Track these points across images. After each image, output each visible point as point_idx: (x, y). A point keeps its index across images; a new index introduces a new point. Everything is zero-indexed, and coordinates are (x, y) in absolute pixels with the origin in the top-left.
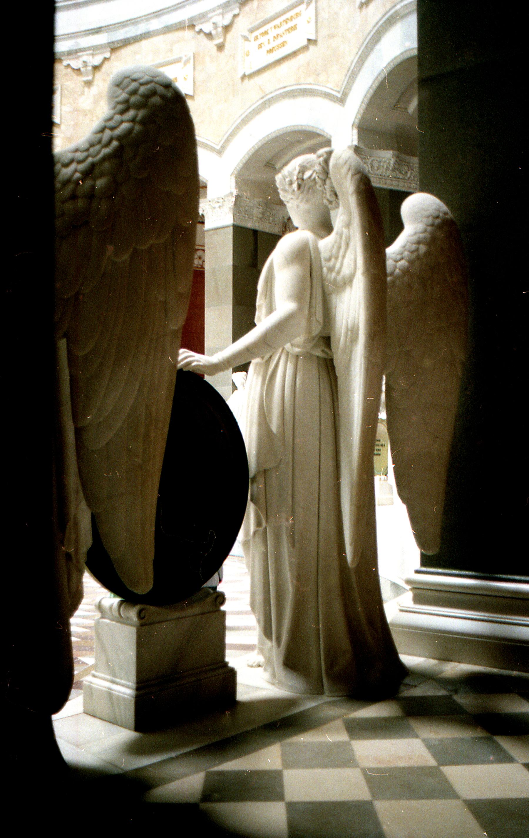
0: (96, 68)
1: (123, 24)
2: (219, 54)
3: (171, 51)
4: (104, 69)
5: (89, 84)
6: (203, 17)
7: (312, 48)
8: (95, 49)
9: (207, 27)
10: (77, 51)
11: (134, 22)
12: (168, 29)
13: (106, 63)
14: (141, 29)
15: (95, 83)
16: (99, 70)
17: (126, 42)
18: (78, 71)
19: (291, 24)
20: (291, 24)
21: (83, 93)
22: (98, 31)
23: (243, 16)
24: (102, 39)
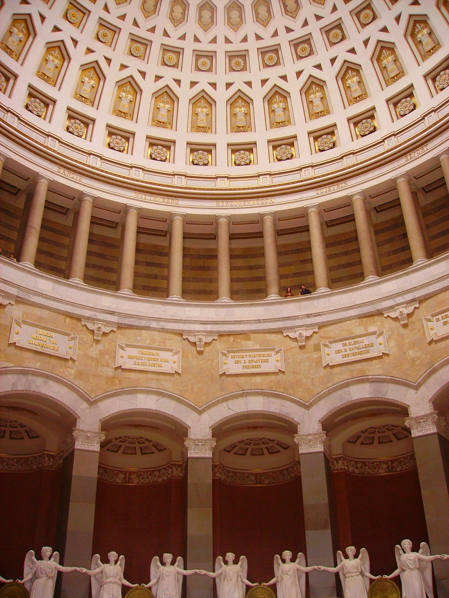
0: (105, 334)
2: (198, 355)
3: (164, 343)
4: (111, 336)
5: (97, 342)
6: (190, 332)
7: (280, 375)
8: (108, 323)
9: (192, 339)
10: (94, 319)
11: (140, 318)
12: (163, 330)
13: (112, 334)
14: (143, 323)
15: (102, 342)
16: (106, 336)
17: (131, 327)
18: (93, 331)
19: (265, 358)
20: (265, 358)
21: (92, 346)
22: (112, 313)
23: (220, 342)
24: (114, 319)
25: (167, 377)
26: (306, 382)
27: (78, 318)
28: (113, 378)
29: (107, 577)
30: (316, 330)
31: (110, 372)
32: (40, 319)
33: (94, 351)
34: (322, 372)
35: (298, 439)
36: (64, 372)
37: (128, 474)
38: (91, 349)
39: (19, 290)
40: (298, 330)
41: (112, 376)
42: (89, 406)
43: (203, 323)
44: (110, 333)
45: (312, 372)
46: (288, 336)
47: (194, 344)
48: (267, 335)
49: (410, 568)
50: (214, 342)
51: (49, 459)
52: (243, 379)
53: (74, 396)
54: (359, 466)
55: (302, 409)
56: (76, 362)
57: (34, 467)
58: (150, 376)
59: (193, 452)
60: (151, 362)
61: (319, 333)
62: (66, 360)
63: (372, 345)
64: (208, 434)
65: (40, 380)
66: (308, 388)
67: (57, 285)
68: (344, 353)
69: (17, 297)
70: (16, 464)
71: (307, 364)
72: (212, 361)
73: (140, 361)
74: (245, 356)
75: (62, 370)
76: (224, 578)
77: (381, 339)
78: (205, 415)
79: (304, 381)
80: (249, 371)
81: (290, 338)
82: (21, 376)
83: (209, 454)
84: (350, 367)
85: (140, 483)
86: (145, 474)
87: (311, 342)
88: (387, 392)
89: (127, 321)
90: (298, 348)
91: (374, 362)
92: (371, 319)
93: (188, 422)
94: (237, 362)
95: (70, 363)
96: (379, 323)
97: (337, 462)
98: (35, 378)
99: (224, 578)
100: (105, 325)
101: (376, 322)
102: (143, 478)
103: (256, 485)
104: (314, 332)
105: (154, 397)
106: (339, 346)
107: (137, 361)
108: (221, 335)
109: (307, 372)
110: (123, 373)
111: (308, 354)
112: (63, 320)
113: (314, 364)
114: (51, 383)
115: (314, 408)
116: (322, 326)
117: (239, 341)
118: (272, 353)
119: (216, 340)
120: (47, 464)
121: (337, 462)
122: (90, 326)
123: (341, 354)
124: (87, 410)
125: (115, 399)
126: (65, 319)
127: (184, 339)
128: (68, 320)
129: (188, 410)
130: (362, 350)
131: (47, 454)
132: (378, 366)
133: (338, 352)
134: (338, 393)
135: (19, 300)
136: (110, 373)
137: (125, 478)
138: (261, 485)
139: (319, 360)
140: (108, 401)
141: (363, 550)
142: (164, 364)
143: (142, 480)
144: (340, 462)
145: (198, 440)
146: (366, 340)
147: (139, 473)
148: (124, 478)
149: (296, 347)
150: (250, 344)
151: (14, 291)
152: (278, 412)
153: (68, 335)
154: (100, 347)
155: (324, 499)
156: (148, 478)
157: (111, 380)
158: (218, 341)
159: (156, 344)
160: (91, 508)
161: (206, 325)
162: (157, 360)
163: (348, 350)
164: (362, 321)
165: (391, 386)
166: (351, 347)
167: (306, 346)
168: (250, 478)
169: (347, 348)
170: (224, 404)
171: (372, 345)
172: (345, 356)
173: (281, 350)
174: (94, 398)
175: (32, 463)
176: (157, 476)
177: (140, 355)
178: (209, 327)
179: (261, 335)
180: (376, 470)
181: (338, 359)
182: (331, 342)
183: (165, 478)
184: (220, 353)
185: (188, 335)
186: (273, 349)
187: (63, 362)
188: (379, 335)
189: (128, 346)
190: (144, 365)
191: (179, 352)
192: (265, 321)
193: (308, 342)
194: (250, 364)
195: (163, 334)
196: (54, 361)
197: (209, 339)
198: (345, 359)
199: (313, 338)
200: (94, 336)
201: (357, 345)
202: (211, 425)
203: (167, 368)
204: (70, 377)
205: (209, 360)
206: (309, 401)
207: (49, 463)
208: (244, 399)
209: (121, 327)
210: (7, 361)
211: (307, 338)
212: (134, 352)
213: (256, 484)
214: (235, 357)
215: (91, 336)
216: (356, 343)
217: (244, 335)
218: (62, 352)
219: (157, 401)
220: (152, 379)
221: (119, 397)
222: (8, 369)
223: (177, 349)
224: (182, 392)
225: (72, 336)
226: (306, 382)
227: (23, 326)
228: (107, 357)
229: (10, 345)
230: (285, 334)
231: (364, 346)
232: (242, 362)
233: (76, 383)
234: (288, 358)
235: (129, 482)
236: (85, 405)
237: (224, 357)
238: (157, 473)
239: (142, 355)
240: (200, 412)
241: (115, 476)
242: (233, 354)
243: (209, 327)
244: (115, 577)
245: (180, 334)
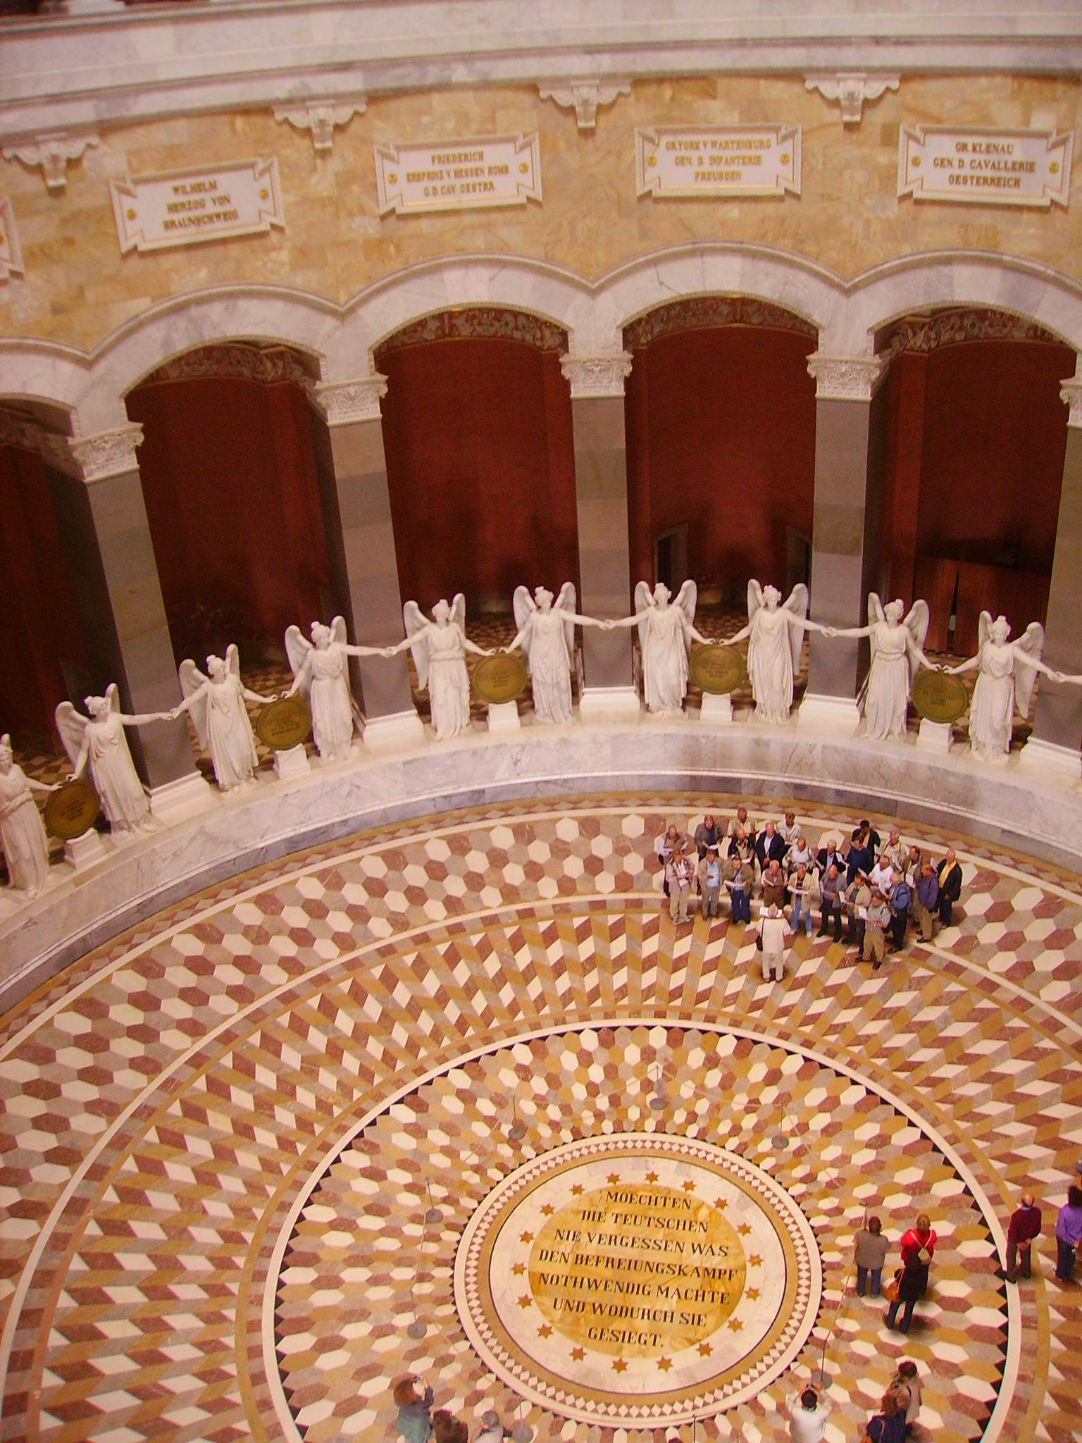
1: (395, 63)
4: (356, 128)
5: (324, 154)
7: (789, 201)
8: (340, 98)
9: (563, 98)
10: (303, 100)
11: (419, 62)
12: (485, 85)
14: (433, 75)
17: (399, 93)
18: (307, 132)
19: (753, 153)
20: (753, 153)
21: (314, 169)
22: (345, 67)
23: (637, 100)
24: (354, 82)
25: (509, 215)
26: (851, 225)
27: (265, 109)
28: (381, 241)
29: (436, 651)
30: (895, 85)
31: (372, 229)
32: (173, 152)
33: (322, 183)
34: (894, 210)
35: (816, 367)
36: (265, 265)
37: (446, 317)
38: (314, 179)
39: (95, 102)
40: (845, 80)
41: (378, 236)
42: (337, 323)
43: (592, 50)
44: (352, 119)
45: (868, 201)
46: (816, 89)
47: (570, 111)
48: (762, 83)
49: (993, 675)
50: (622, 100)
51: (274, 365)
52: (695, 208)
53: (302, 312)
54: (967, 322)
55: (835, 295)
56: (288, 231)
57: (246, 372)
58: (467, 220)
59: (580, 385)
60: (465, 181)
61: (900, 92)
62: (261, 235)
63: (1030, 167)
64: (615, 343)
65: (216, 310)
66: (853, 242)
67: (184, 29)
68: (955, 171)
69: (100, 122)
70: (205, 361)
71: (860, 176)
72: (619, 157)
73: (438, 184)
74: (701, 146)
75: (260, 263)
76: (651, 631)
77: (1057, 155)
78: (606, 298)
79: (846, 221)
80: (709, 188)
81: (822, 96)
82: (173, 318)
83: (617, 390)
84: (963, 212)
85: (475, 333)
86: (485, 315)
87: (878, 117)
88: (1038, 303)
89: (388, 80)
90: (841, 127)
91: (1026, 216)
92: (1047, 88)
93: (566, 319)
94: (681, 162)
95: (274, 237)
96: (1063, 107)
97: (915, 334)
98: (206, 309)
99: (651, 631)
100: (333, 106)
101: (1055, 100)
102: (480, 324)
103: (732, 325)
104: (888, 90)
105: (484, 273)
106: (944, 146)
107: (430, 184)
108: (639, 81)
109: (857, 198)
110: (401, 224)
111: (866, 150)
112: (227, 129)
113: (877, 181)
114: (243, 304)
115: (860, 296)
116: (908, 75)
117: (687, 97)
118: (772, 137)
119: (627, 96)
120: (273, 373)
121: (915, 334)
122: (299, 118)
123: (948, 172)
124: (337, 333)
125: (393, 293)
126: (233, 124)
127: (544, 101)
128: (240, 122)
129: (566, 289)
130: (1003, 174)
131: (266, 355)
132: (1032, 231)
133: (941, 163)
134: (923, 274)
135: (105, 129)
136: (371, 231)
137: (441, 328)
138: (742, 325)
139: (888, 176)
140: (378, 303)
141: (919, 606)
142: (498, 180)
143: (479, 329)
144: (921, 335)
145: (592, 360)
146: (1019, 151)
147: (470, 314)
148: (439, 328)
149: (835, 124)
150: (716, 110)
151: (84, 112)
152: (776, 297)
153: (252, 166)
154: (334, 165)
155: (859, 499)
156: (492, 325)
157: (376, 247)
158: (632, 99)
159: (474, 127)
160: (386, 530)
161: (598, 57)
162: (477, 172)
163: (967, 163)
164: (1020, 86)
165: (1053, 293)
166: (982, 157)
167: (863, 125)
168: (720, 310)
169: (968, 157)
170: (650, 273)
171: (1030, 167)
172: (955, 180)
173: (795, 132)
174: (347, 303)
175: (239, 362)
176: (512, 325)
177: (437, 167)
178: (606, 63)
179: (747, 84)
180: (1006, 331)
181: (935, 184)
182: (926, 132)
183: (528, 337)
184: (636, 135)
185: (551, 88)
186: (776, 130)
187: (256, 243)
188: (1055, 146)
189: (399, 149)
190: (451, 190)
191: (533, 140)
192: (759, 43)
193: (868, 113)
194: (715, 169)
195: (487, 96)
196: (234, 249)
197: (608, 95)
198: (955, 187)
199: (883, 105)
200: (312, 142)
201: (994, 157)
202: (619, 323)
203: (506, 191)
204: (282, 271)
205: (609, 152)
206: (852, 279)
207: (276, 372)
208: (697, 261)
209: (374, 98)
210: (133, 293)
211: (868, 104)
212: (420, 161)
213: (731, 322)
214: (677, 146)
215: (306, 142)
216: (992, 148)
217: (703, 83)
218: (248, 222)
219: (491, 279)
220: (473, 227)
221: (403, 287)
222: (142, 317)
223: (528, 130)
224: (549, 248)
225: (261, 165)
226: (851, 225)
227: (142, 191)
228: (356, 188)
229: (126, 256)
230: (809, 85)
231: (1009, 165)
232: (695, 161)
233: (299, 279)
234: (813, 156)
235: (450, 334)
236: (329, 323)
237: (648, 146)
238: (510, 319)
239: (444, 168)
240: (594, 293)
241: (420, 328)
242: (670, 138)
243: (606, 63)
244: (451, 649)
245: (532, 87)
